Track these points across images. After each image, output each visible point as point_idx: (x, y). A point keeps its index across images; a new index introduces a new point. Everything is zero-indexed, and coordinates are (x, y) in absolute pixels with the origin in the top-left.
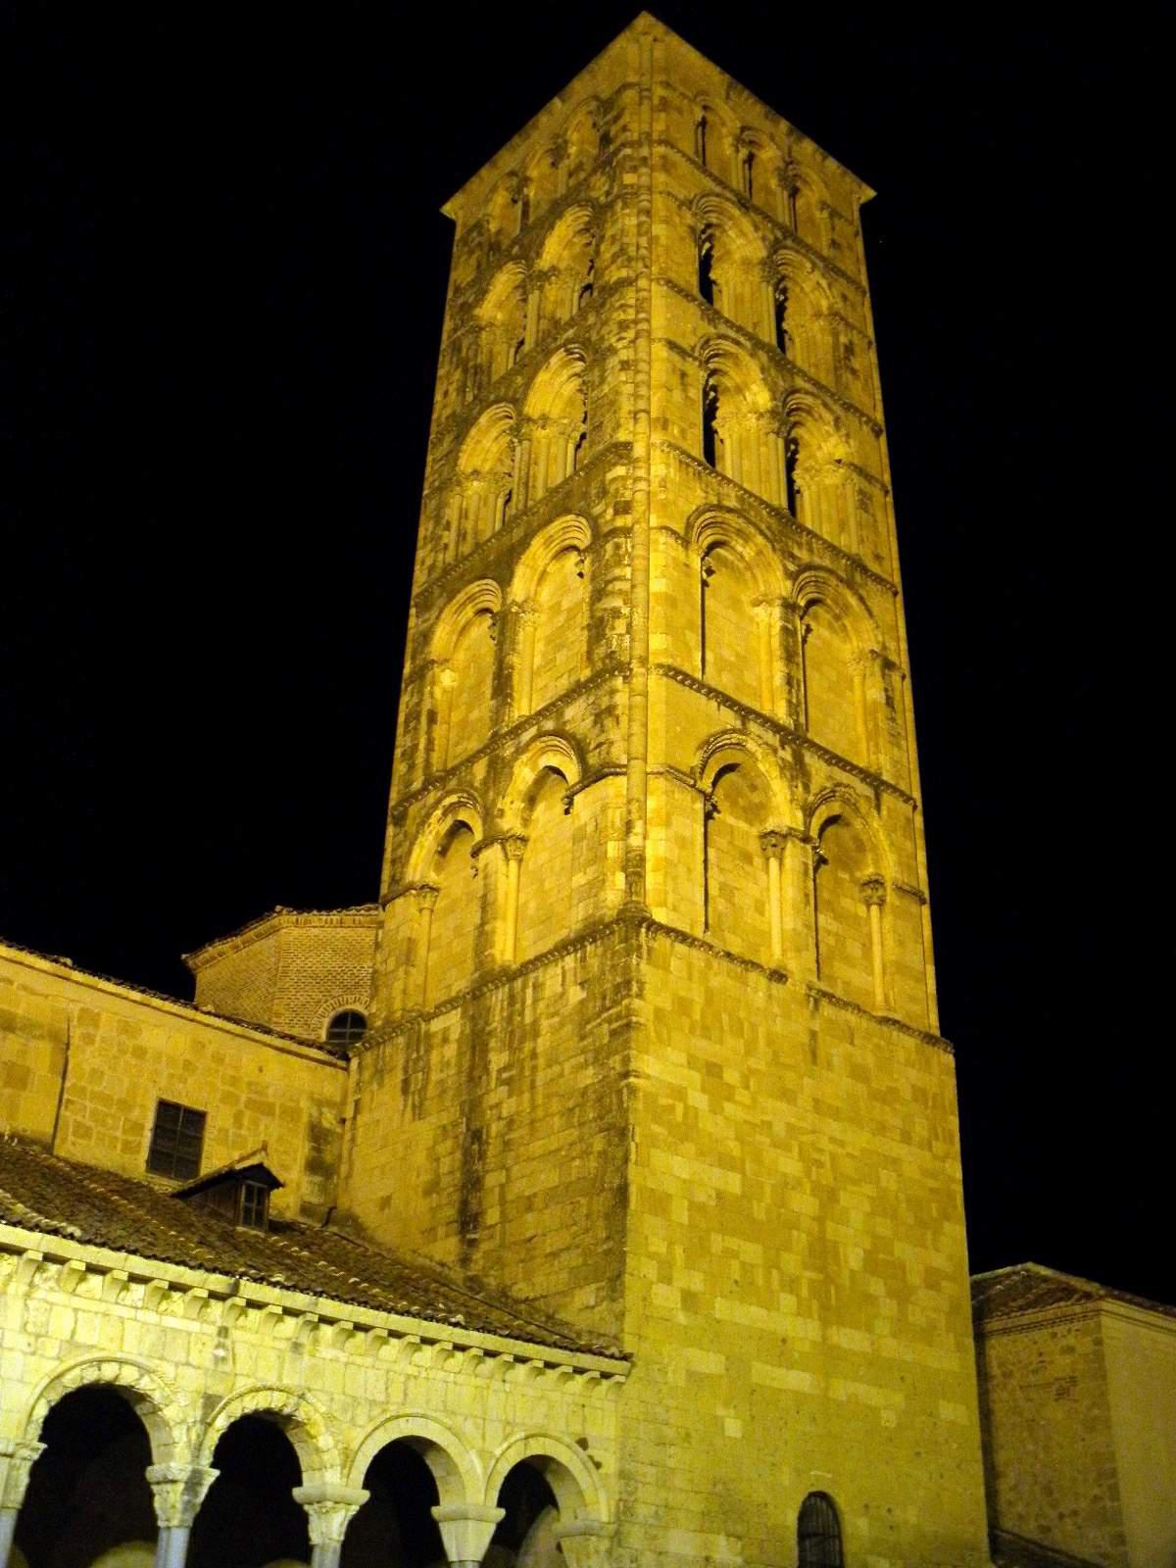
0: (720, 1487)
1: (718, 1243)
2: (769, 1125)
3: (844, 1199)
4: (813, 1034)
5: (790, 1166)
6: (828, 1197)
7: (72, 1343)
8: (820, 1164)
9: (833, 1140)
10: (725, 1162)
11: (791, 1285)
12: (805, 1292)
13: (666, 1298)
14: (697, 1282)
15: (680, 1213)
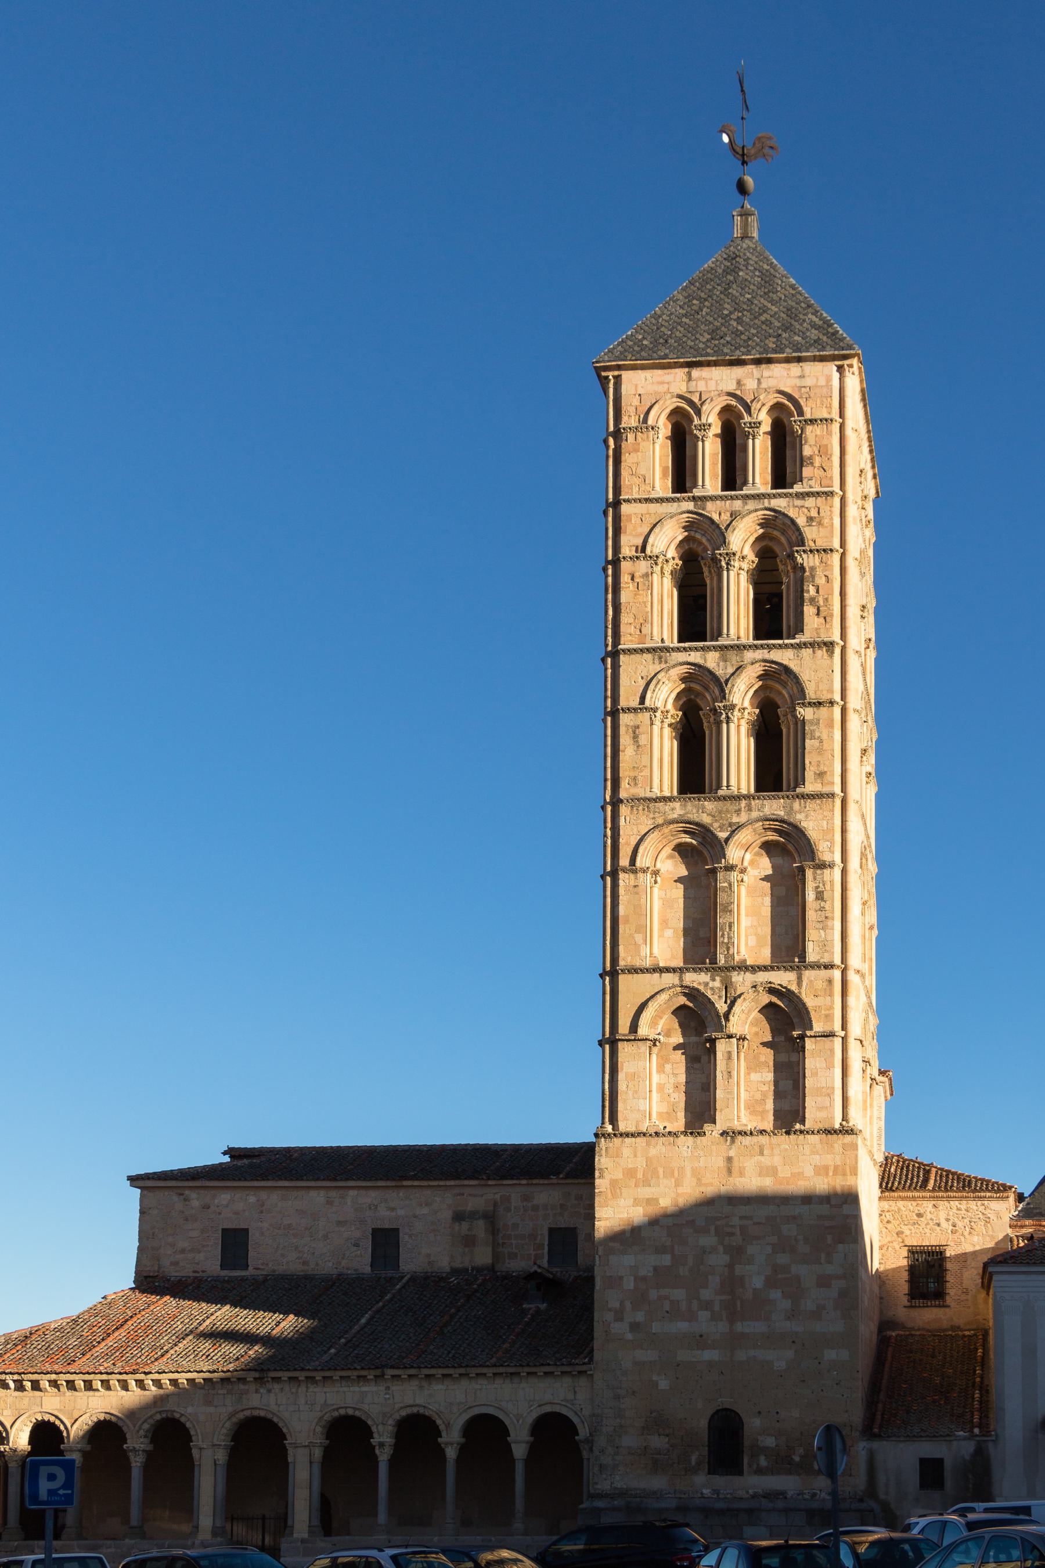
0: (654, 1414)
1: (653, 1294)
2: (693, 1222)
3: (751, 1250)
4: (729, 1159)
5: (708, 1240)
6: (737, 1253)
7: (325, 1404)
8: (732, 1234)
9: (741, 1218)
10: (661, 1250)
11: (707, 1305)
12: (717, 1308)
13: (619, 1328)
14: (640, 1317)
15: (629, 1284)
